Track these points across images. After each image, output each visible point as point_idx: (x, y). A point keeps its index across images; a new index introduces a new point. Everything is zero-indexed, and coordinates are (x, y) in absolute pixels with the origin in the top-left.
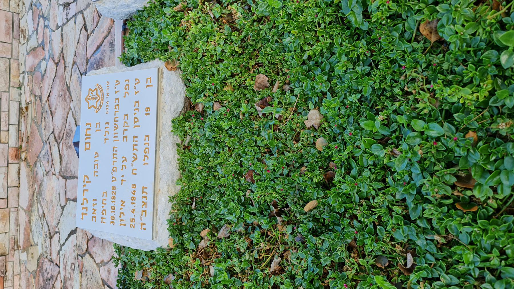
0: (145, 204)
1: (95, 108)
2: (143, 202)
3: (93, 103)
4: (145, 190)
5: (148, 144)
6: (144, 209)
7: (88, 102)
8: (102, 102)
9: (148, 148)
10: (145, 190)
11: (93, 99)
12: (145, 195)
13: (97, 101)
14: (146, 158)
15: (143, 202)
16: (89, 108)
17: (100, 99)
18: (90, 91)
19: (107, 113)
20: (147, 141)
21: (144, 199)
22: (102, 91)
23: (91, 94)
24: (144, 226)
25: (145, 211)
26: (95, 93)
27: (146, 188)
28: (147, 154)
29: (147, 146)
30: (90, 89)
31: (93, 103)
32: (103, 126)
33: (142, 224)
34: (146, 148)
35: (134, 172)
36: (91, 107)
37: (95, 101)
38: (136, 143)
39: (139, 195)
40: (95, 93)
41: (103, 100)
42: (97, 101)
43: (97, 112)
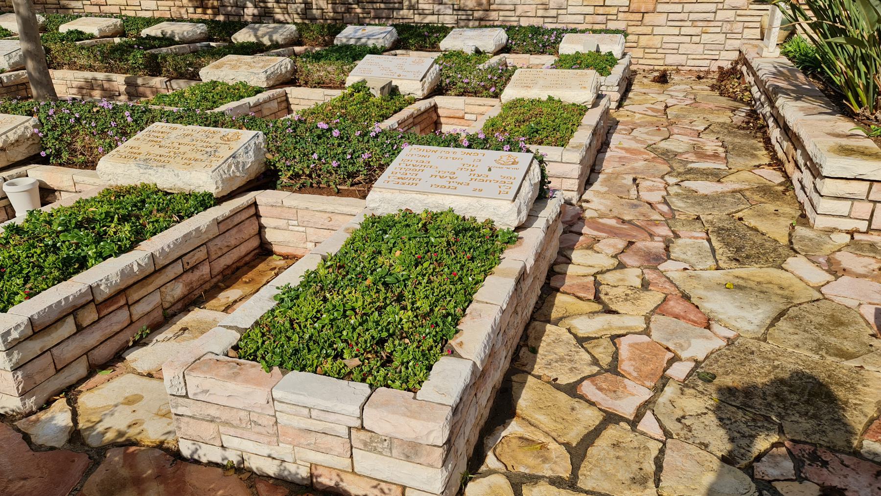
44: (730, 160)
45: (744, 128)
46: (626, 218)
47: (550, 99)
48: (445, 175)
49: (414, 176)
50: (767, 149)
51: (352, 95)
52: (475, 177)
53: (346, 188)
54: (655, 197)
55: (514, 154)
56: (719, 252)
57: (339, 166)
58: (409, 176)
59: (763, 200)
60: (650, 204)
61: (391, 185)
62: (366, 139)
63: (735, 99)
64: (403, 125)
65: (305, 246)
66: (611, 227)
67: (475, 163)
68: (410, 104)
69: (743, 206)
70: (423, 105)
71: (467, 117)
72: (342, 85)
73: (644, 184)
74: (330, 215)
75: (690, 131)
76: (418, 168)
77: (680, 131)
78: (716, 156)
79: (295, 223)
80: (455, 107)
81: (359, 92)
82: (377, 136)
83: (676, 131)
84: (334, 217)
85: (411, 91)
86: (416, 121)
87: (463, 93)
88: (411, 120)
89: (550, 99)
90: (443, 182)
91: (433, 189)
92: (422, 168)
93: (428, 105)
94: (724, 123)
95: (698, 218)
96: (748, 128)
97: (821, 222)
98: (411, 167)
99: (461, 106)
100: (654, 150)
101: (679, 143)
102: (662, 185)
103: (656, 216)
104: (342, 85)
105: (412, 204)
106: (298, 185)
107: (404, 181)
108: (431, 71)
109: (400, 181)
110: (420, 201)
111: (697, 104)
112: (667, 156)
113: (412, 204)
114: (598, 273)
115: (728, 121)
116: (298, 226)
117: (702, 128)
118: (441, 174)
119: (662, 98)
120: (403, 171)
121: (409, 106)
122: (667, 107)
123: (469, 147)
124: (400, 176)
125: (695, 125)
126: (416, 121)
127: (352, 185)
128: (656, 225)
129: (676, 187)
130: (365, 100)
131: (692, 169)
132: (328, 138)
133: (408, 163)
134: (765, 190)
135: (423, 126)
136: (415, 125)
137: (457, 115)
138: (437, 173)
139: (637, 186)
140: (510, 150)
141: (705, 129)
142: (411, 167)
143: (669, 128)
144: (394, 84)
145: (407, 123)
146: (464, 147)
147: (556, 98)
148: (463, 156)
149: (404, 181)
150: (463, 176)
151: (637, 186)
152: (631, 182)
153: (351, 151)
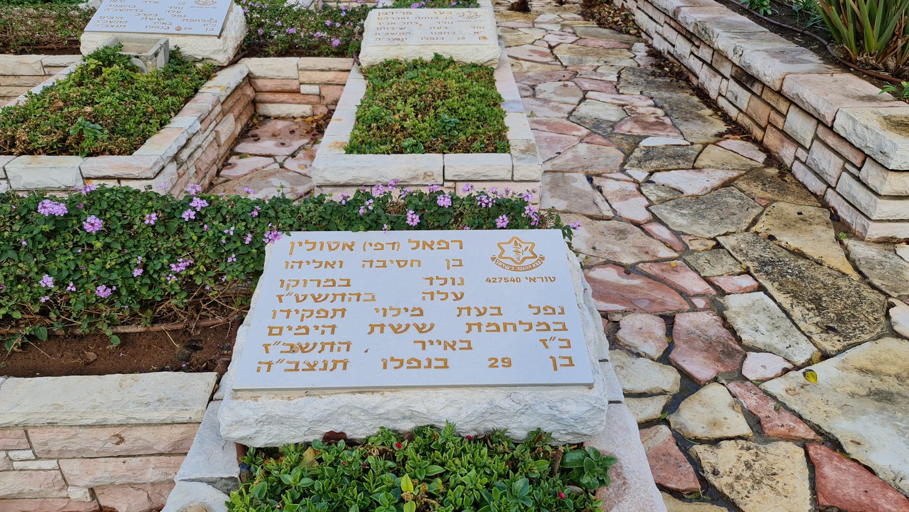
1: (500, 256)
3: (509, 251)
5: (429, 366)
7: (509, 243)
8: (510, 269)
9: (419, 367)
13: (513, 260)
16: (499, 245)
18: (530, 246)
19: (488, 280)
20: (434, 363)
23: (524, 246)
29: (425, 363)
30: (533, 244)
31: (509, 251)
33: (270, 364)
34: (419, 362)
36: (502, 249)
37: (513, 255)
41: (515, 270)
42: (513, 260)
43: (493, 259)
44: (681, 128)
45: (660, 76)
46: (628, 260)
47: (438, 58)
48: (404, 319)
49: (328, 337)
50: (709, 107)
51: (98, 72)
52: (474, 319)
53: (140, 329)
54: (635, 209)
55: (525, 235)
56: (797, 312)
57: (117, 293)
58: (314, 337)
59: (777, 198)
60: (638, 225)
61: (280, 378)
62: (175, 224)
63: (620, 32)
64: (207, 121)
65: (64, 494)
66: (618, 287)
67: (456, 273)
68: (209, 78)
69: (756, 211)
70: (230, 78)
71: (304, 89)
72: (73, 48)
73: (609, 186)
74: (118, 431)
75: (602, 84)
76: (327, 305)
77: (593, 86)
78: (660, 124)
79: (29, 454)
80: (283, 75)
81: (110, 64)
82: (200, 216)
83: (587, 85)
84: (131, 435)
85: (206, 55)
86: (226, 107)
87: (290, 50)
88: (218, 108)
89: (438, 58)
90: (405, 346)
91: (392, 377)
92: (338, 304)
93: (239, 78)
94: (633, 68)
95: (718, 246)
96: (666, 75)
97: (876, 231)
98: (309, 304)
99: (293, 74)
100: (581, 122)
101: (602, 107)
102: (632, 187)
103: (664, 253)
104: (73, 48)
105: (344, 419)
106: (19, 340)
107: (312, 357)
108: (231, 17)
109: (299, 356)
110: (365, 412)
111: (583, 42)
112: (599, 129)
113: (344, 419)
114: (666, 409)
115: (635, 65)
116: (37, 458)
117: (614, 78)
118: (389, 320)
119: (537, 34)
120: (294, 320)
121: (209, 83)
122: (551, 48)
123: (419, 227)
124: (295, 340)
125: (602, 74)
126: (226, 107)
127: (154, 321)
128: (675, 270)
129: (651, 187)
130: (127, 81)
131: (648, 150)
132: (75, 233)
133: (300, 290)
134: (752, 174)
135: (236, 112)
136: (224, 113)
137: (287, 88)
138: (379, 319)
139: (601, 192)
140: (510, 226)
141: (619, 77)
142: (309, 304)
143: (575, 80)
144: (171, 47)
145: (212, 116)
146: (409, 228)
147: (446, 57)
148: (420, 253)
149: (312, 357)
150: (446, 321)
151: (601, 192)
152: (588, 187)
153: (140, 259)
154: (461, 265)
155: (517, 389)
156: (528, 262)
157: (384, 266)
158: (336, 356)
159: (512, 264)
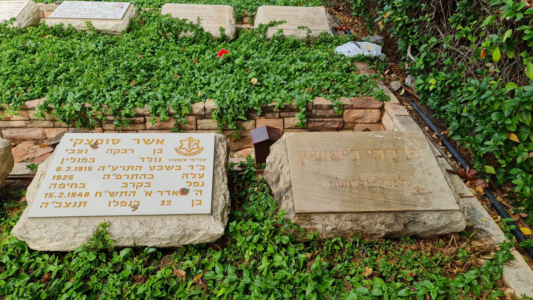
0: (68, 205)
2: (70, 203)
4: (83, 204)
6: (64, 204)
10: (83, 204)
11: (189, 146)
12: (78, 204)
14: (116, 204)
15: (70, 203)
17: (189, 153)
21: (73, 204)
22: (195, 154)
23: (194, 142)
24: (44, 205)
25: (60, 206)
26: (195, 146)
27: (84, 206)
28: (120, 204)
31: (186, 145)
32: (157, 156)
35: (99, 194)
38: (128, 194)
39: (78, 199)
40: (195, 146)
43: (175, 149)
154: (161, 152)
155: (68, 219)
156: (194, 151)
157: (126, 152)
158: (83, 199)
159: (186, 152)
